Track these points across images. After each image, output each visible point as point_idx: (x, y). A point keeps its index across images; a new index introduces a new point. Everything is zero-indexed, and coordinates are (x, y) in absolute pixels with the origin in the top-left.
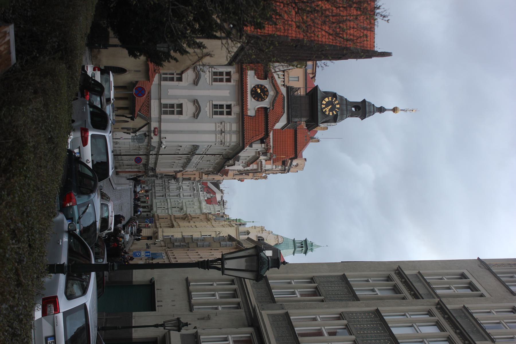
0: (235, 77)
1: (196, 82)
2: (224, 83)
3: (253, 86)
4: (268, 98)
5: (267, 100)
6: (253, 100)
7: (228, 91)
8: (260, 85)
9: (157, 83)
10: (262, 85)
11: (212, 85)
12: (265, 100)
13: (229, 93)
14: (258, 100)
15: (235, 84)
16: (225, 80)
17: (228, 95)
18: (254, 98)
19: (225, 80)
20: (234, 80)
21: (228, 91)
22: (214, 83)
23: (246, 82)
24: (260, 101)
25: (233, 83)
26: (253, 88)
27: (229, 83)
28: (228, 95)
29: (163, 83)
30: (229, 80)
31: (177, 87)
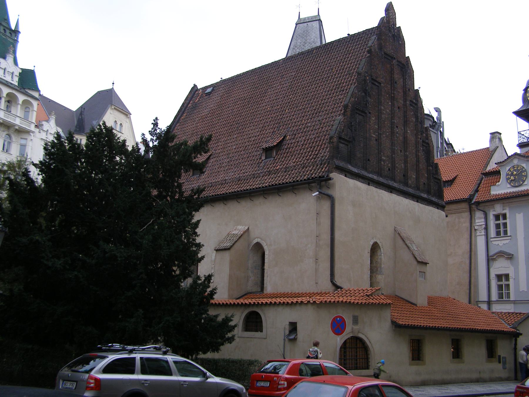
0: (498, 209)
1: (510, 257)
2: (508, 221)
3: (509, 186)
4: (522, 165)
5: (524, 165)
6: (525, 183)
7: (517, 215)
8: (507, 176)
9: (512, 305)
10: (507, 175)
11: (510, 236)
12: (523, 167)
13: (519, 213)
14: (526, 176)
15: (508, 208)
16: (504, 221)
17: (522, 214)
18: (524, 181)
19: (504, 221)
20: (503, 210)
21: (517, 215)
22: (509, 234)
23: (504, 194)
24: (526, 173)
25: (507, 211)
26: (511, 185)
27: (508, 216)
28: (522, 214)
29: (512, 298)
30: (504, 216)
31: (517, 279)
